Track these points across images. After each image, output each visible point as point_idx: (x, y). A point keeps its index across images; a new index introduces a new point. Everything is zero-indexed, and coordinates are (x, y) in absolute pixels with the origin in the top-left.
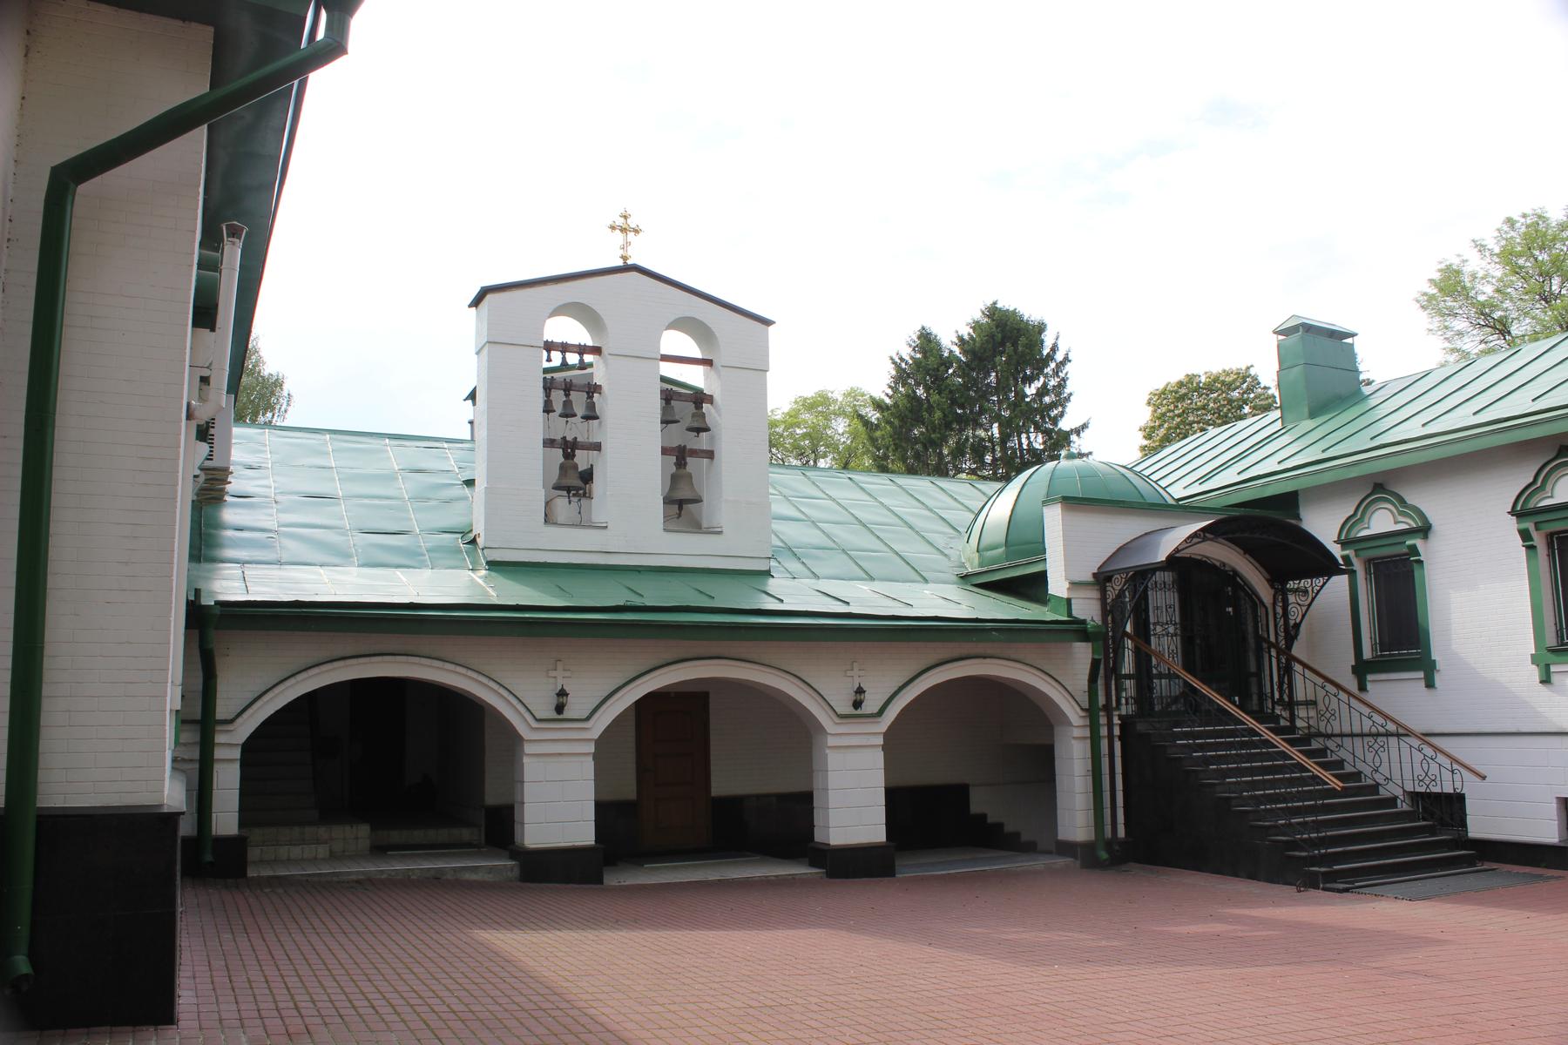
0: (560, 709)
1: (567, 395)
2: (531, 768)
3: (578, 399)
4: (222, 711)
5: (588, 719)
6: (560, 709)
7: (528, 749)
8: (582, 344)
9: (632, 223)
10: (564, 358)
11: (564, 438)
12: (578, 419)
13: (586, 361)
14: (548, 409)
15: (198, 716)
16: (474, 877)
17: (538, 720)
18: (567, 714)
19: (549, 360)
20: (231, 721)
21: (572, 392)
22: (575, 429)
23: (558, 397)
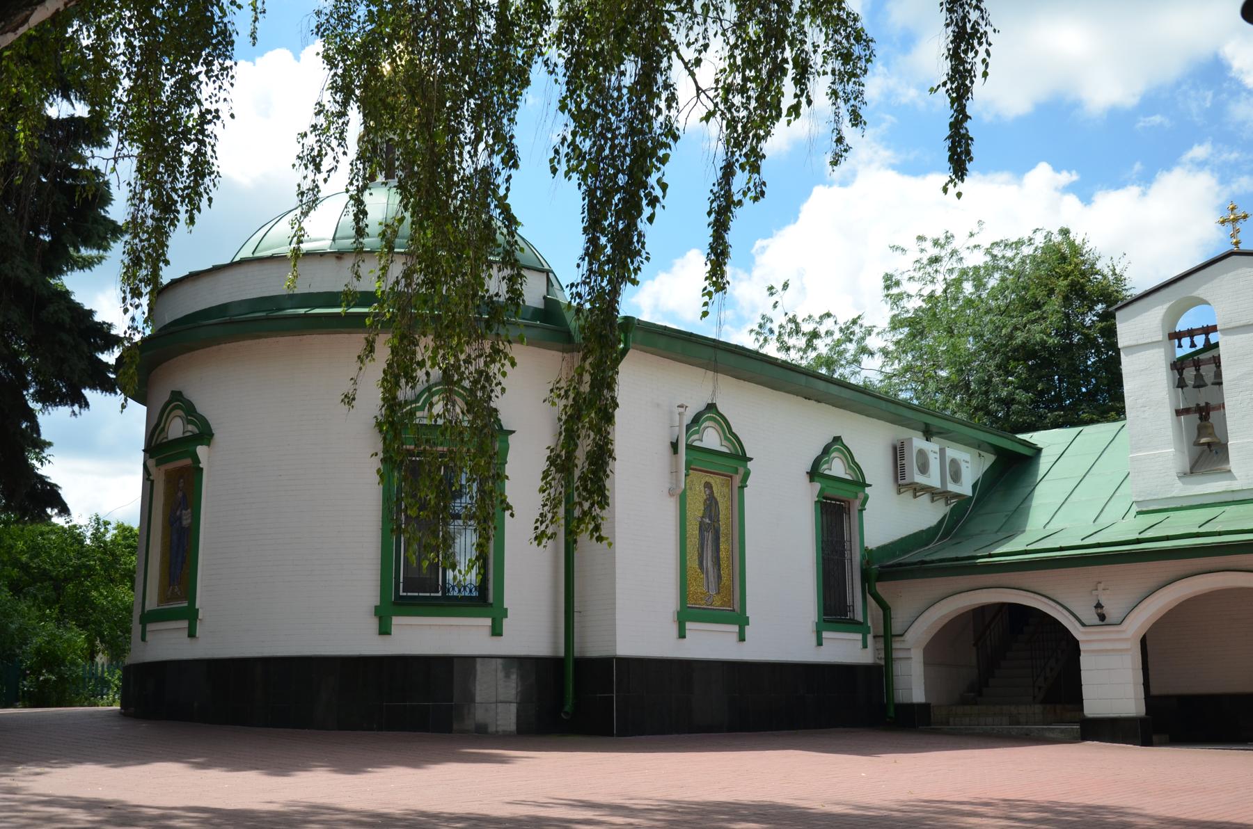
0: (1102, 617)
1: (1198, 370)
2: (1085, 661)
3: (1207, 371)
4: (896, 627)
5: (1120, 624)
6: (1102, 617)
7: (1082, 647)
8: (1205, 326)
9: (1239, 213)
10: (1207, 340)
11: (1198, 405)
12: (1210, 386)
13: (1212, 342)
14: (1181, 384)
15: (882, 633)
16: (1052, 735)
17: (1083, 625)
18: (1107, 621)
19: (1193, 345)
20: (902, 635)
21: (1202, 367)
22: (1203, 397)
23: (1190, 373)
